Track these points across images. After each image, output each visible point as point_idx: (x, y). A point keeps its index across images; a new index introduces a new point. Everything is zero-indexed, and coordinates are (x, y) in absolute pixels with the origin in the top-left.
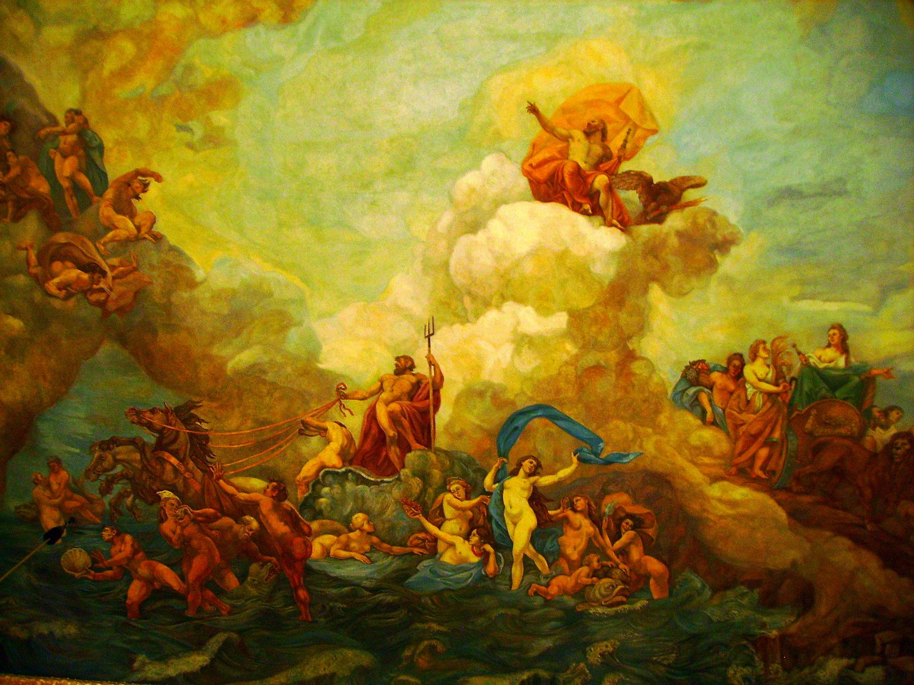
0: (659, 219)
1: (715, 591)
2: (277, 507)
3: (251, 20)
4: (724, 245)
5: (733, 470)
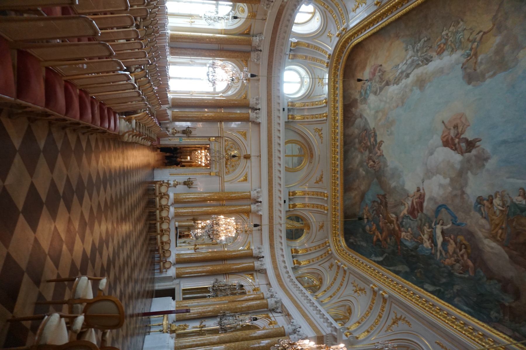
0: (470, 152)
1: (488, 279)
2: (397, 223)
3: (397, 106)
4: (486, 159)
5: (491, 236)
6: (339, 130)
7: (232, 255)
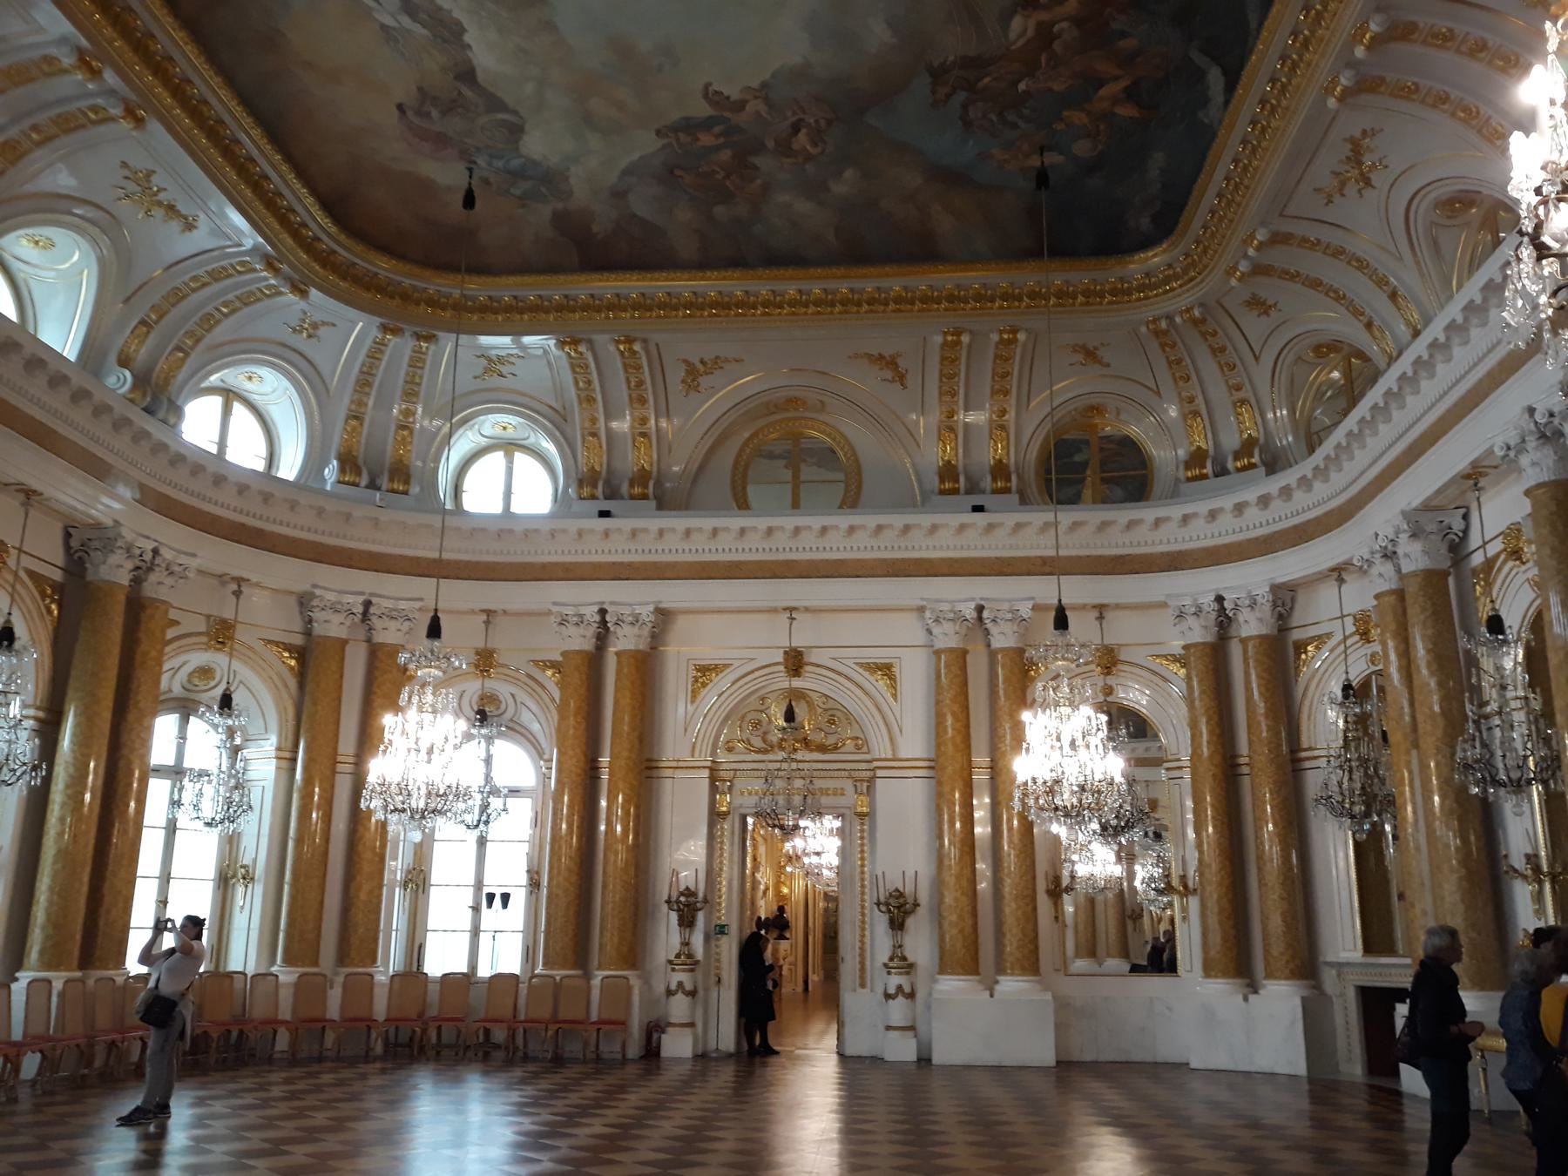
3: (550, 27)
6: (684, 285)
7: (1211, 733)
